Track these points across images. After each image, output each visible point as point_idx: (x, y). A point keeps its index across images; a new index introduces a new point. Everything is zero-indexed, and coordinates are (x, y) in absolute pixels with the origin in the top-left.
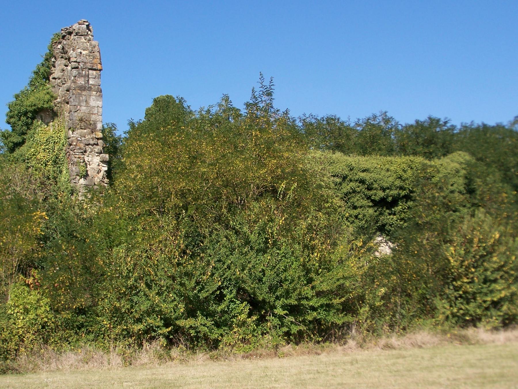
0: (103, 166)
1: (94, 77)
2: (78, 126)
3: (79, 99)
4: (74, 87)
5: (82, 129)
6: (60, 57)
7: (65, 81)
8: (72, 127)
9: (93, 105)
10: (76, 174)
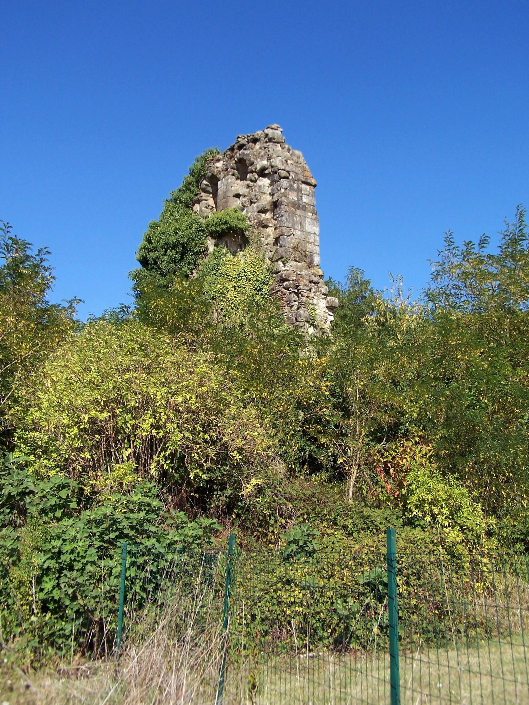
0: (329, 315)
1: (308, 193)
2: (292, 257)
3: (293, 220)
4: (286, 203)
5: (295, 261)
6: (231, 173)
7: (257, 199)
8: (284, 256)
9: (309, 231)
10: (304, 320)
